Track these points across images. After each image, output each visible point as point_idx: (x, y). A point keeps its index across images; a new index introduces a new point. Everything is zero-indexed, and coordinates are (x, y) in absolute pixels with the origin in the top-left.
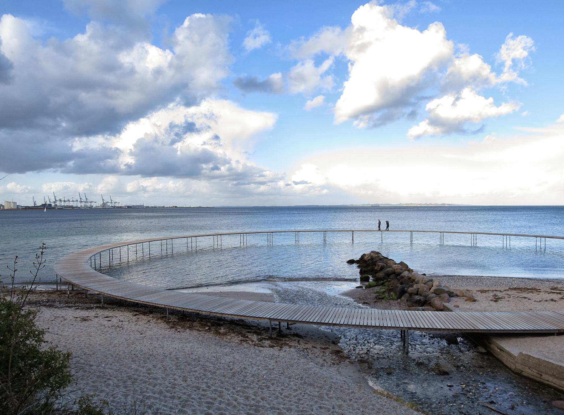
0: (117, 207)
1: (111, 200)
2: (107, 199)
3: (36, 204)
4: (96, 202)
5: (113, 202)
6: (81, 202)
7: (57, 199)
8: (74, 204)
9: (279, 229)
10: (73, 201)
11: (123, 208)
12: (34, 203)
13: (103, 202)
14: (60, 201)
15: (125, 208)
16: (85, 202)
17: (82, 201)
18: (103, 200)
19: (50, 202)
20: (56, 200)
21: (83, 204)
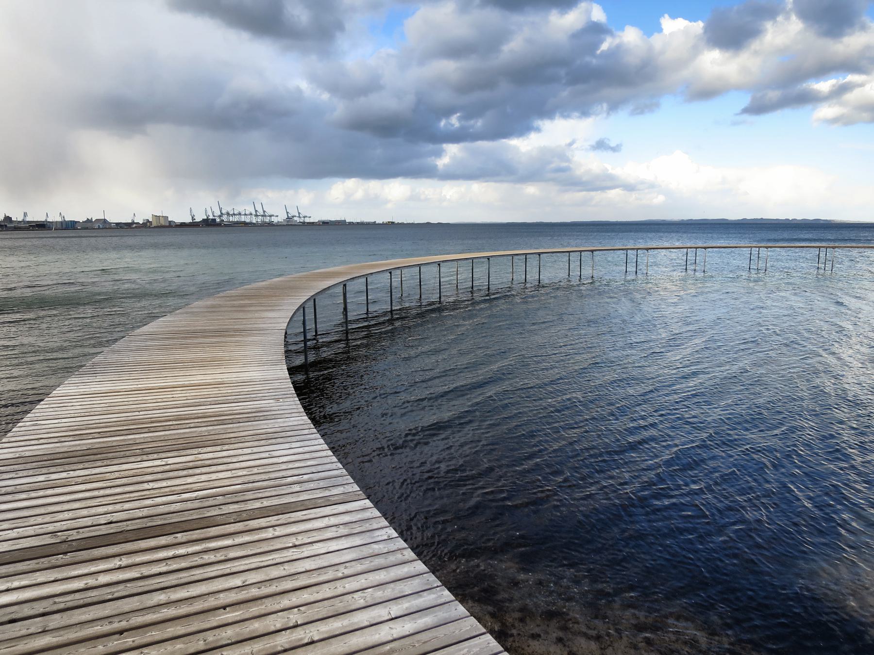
0: (308, 223)
1: (299, 213)
2: (293, 212)
3: (195, 219)
4: (277, 216)
5: (301, 216)
6: (256, 215)
7: (224, 212)
8: (247, 220)
9: (667, 245)
10: (245, 215)
11: (316, 225)
12: (192, 218)
13: (288, 216)
14: (228, 214)
15: (319, 225)
16: (262, 216)
17: (258, 214)
18: (287, 213)
19: (214, 216)
20: (221, 213)
21: (260, 219)
